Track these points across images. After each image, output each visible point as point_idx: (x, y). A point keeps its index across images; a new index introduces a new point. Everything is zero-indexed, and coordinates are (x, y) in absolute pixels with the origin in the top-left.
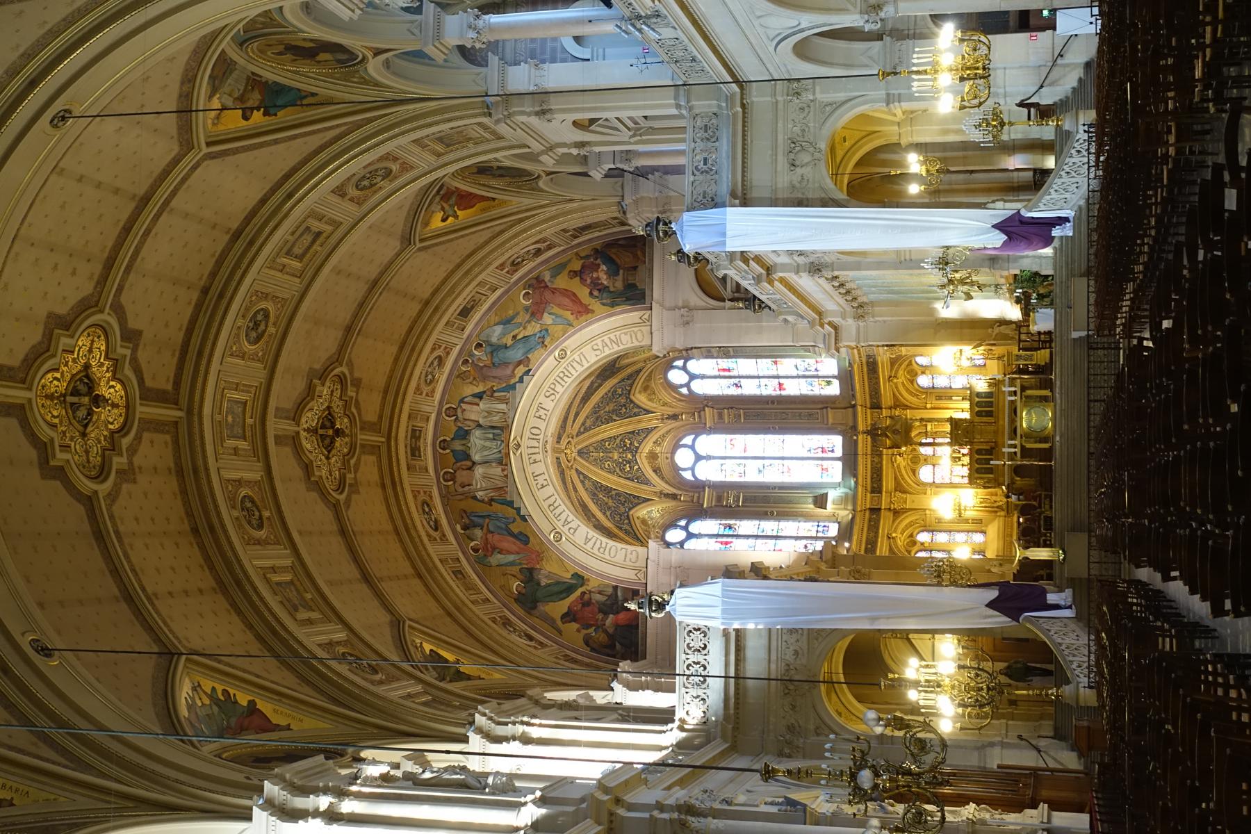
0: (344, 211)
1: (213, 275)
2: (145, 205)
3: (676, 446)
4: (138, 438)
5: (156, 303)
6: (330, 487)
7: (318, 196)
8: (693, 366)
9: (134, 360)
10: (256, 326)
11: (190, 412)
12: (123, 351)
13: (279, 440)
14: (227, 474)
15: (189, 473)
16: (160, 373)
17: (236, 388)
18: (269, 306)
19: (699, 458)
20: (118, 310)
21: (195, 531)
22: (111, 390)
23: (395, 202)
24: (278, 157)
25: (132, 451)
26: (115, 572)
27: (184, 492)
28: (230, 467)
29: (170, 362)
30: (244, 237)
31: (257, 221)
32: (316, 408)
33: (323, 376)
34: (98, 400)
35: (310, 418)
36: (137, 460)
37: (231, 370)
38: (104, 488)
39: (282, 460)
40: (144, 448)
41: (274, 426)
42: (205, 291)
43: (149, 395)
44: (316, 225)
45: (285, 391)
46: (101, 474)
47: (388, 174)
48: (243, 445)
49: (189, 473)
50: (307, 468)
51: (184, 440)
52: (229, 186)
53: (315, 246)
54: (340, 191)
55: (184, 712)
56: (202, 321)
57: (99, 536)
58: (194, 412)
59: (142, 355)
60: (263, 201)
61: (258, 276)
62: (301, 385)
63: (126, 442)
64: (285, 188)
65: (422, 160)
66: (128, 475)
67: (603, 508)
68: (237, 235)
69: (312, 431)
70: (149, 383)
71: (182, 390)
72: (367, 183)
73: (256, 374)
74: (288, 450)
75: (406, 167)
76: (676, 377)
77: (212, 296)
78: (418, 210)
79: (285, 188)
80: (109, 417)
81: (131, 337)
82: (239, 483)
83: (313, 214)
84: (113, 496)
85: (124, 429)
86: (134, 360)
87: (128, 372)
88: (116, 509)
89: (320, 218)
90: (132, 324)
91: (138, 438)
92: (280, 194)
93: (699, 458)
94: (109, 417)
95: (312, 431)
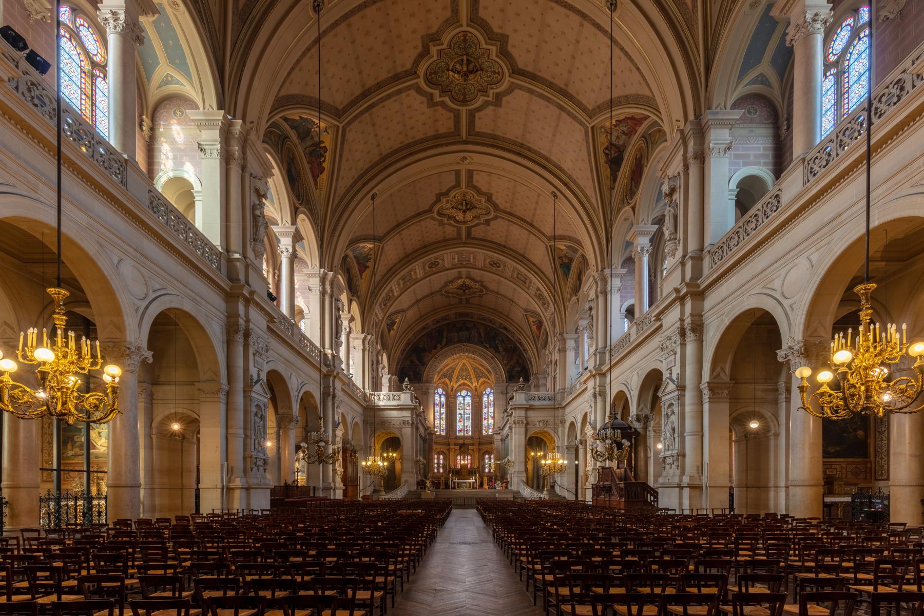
0: (532, 291)
1: (510, 249)
2: (530, 225)
3: (468, 391)
4: (454, 226)
5: (499, 230)
6: (446, 289)
7: (537, 282)
8: (491, 395)
9: (480, 224)
10: (494, 264)
11: (465, 243)
12: (482, 220)
13: (460, 272)
14: (445, 256)
15: (444, 243)
16: (478, 232)
17: (475, 258)
18: (501, 268)
19: (464, 397)
20: (496, 218)
21: (425, 246)
22: (469, 215)
23: (536, 306)
24: (548, 269)
25: (450, 224)
26: (407, 220)
27: (438, 242)
28: (448, 257)
29: (481, 236)
30: (523, 258)
31: (528, 263)
32: (472, 284)
33: (482, 285)
34: (465, 212)
35: (468, 282)
36: (447, 226)
37: (481, 256)
38: (435, 215)
39: (453, 273)
40: (451, 228)
41: (464, 271)
42: (505, 247)
43: (469, 229)
44: (527, 282)
45: (476, 274)
46: (440, 214)
47: (544, 304)
48: (456, 260)
49: (444, 243)
50: (452, 282)
51: (456, 241)
52: (539, 253)
53: (522, 281)
54: (538, 289)
55: (361, 245)
56: (495, 246)
57: (418, 215)
58: (465, 244)
59: (482, 227)
60: (534, 264)
61: (511, 264)
62: (478, 278)
63: (452, 222)
64: (539, 272)
65: (548, 314)
66: (441, 223)
67: (448, 371)
68: (523, 256)
69: (464, 283)
70: (473, 229)
71: (471, 240)
72: (540, 297)
73: (480, 265)
74: (457, 275)
75: (546, 309)
76: (488, 390)
77: (503, 248)
78: (535, 314)
79: (539, 272)
80: (460, 216)
81: (487, 223)
82: (443, 260)
83: (531, 281)
84: (433, 218)
85: (456, 221)
86: (480, 224)
87: (476, 222)
88: (429, 220)
89: (530, 283)
90: (492, 223)
91: (454, 226)
92: (536, 270)
93: (464, 397)
94: (460, 216)
95: (464, 283)
